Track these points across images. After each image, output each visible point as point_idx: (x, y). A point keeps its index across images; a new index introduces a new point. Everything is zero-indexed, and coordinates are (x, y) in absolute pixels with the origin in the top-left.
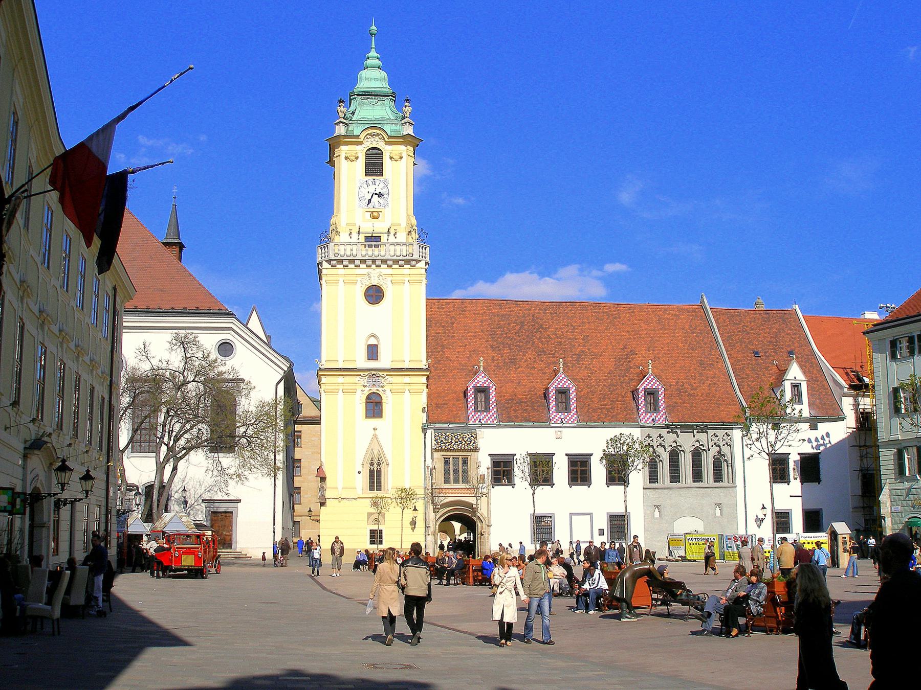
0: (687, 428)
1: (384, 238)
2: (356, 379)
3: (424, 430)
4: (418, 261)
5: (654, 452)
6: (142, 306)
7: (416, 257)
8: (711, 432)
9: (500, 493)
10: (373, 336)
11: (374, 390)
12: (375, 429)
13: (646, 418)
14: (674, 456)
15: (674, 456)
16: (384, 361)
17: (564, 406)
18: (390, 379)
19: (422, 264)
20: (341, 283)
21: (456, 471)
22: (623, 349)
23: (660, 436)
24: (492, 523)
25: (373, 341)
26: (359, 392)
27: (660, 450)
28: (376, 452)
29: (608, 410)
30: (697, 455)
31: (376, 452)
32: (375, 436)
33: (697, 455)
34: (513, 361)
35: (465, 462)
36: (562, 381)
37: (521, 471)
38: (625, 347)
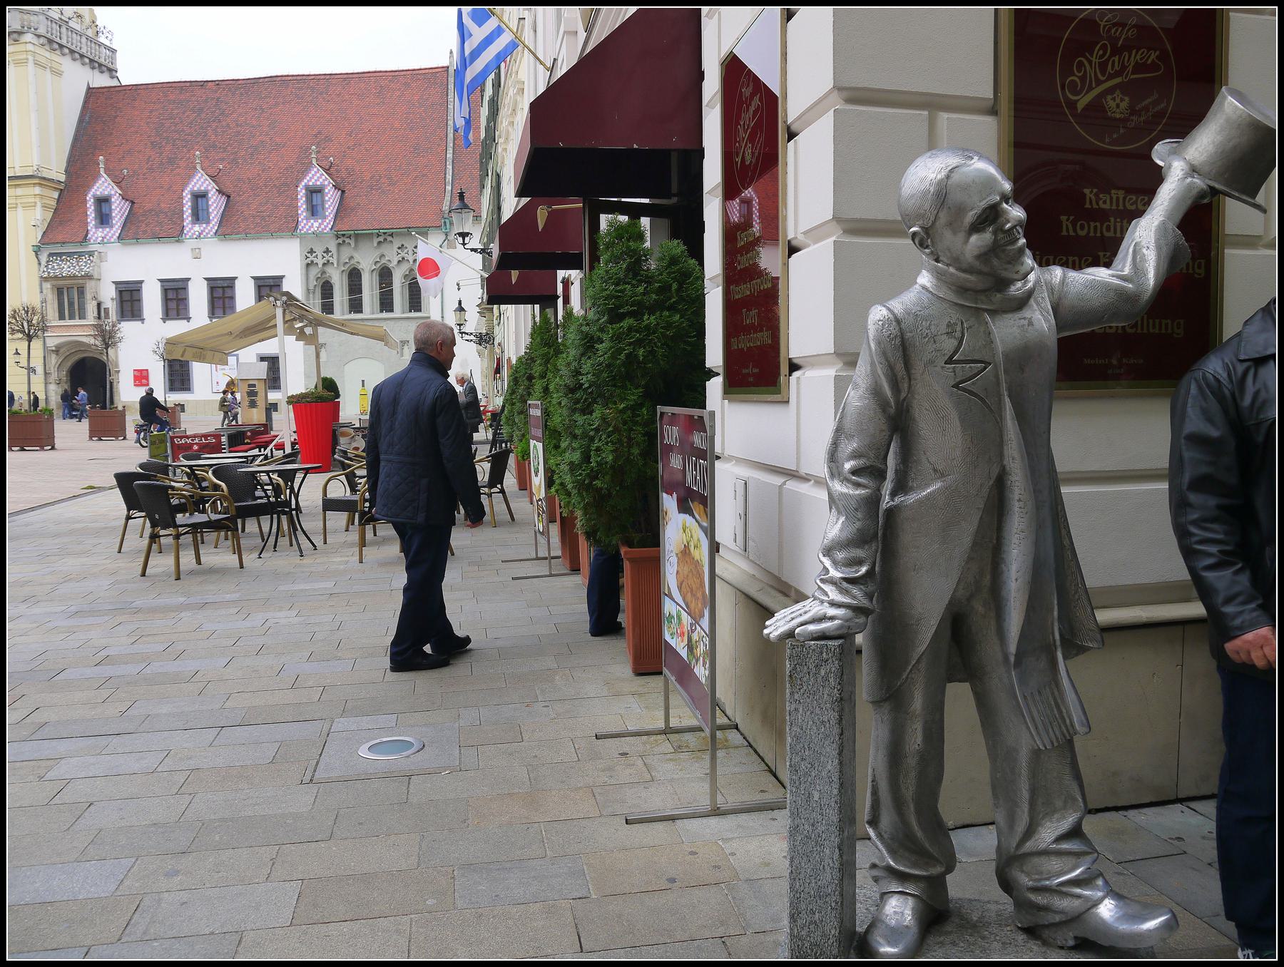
0: (358, 237)
3: (37, 252)
4: (20, 33)
5: (324, 272)
8: (397, 243)
9: (128, 329)
13: (309, 225)
14: (354, 277)
15: (354, 277)
17: (197, 217)
19: (28, 37)
21: (71, 304)
22: (316, 136)
23: (327, 251)
24: (121, 368)
27: (329, 270)
29: (263, 218)
30: (385, 275)
33: (385, 275)
34: (171, 161)
35: (81, 291)
36: (201, 182)
37: (152, 300)
38: (319, 133)
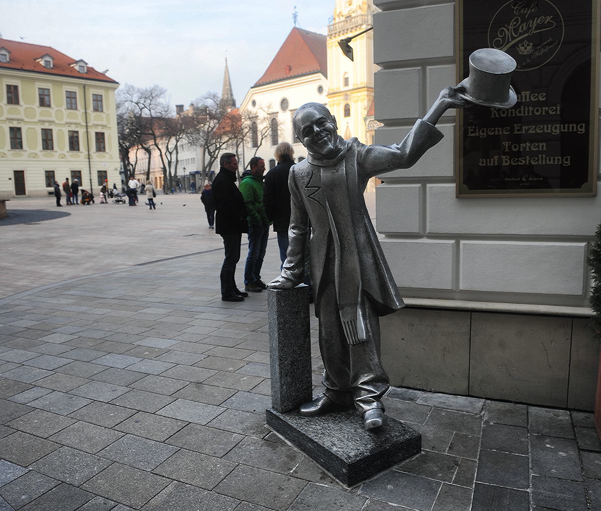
1: (353, 15)
2: (339, 98)
3: (365, 119)
4: (361, 25)
6: (292, 75)
7: (360, 22)
10: (346, 73)
11: (346, 102)
12: (348, 123)
16: (350, 87)
18: (354, 95)
20: (334, 47)
25: (346, 77)
26: (341, 104)
28: (348, 135)
31: (348, 135)
32: (348, 126)
